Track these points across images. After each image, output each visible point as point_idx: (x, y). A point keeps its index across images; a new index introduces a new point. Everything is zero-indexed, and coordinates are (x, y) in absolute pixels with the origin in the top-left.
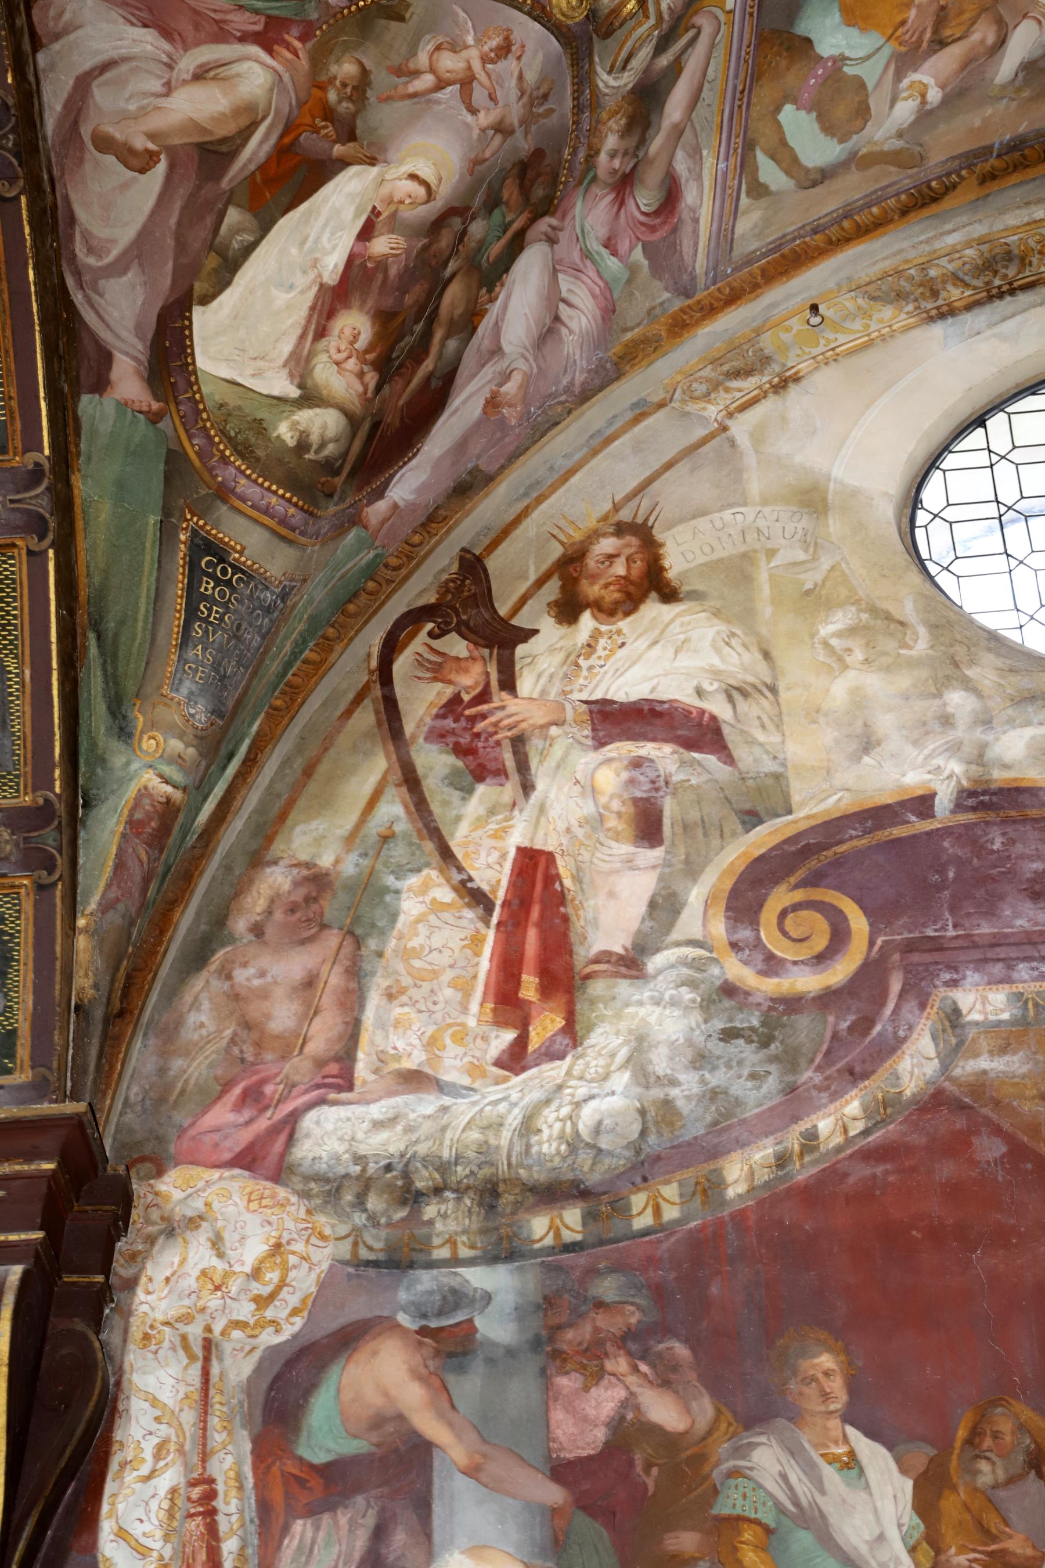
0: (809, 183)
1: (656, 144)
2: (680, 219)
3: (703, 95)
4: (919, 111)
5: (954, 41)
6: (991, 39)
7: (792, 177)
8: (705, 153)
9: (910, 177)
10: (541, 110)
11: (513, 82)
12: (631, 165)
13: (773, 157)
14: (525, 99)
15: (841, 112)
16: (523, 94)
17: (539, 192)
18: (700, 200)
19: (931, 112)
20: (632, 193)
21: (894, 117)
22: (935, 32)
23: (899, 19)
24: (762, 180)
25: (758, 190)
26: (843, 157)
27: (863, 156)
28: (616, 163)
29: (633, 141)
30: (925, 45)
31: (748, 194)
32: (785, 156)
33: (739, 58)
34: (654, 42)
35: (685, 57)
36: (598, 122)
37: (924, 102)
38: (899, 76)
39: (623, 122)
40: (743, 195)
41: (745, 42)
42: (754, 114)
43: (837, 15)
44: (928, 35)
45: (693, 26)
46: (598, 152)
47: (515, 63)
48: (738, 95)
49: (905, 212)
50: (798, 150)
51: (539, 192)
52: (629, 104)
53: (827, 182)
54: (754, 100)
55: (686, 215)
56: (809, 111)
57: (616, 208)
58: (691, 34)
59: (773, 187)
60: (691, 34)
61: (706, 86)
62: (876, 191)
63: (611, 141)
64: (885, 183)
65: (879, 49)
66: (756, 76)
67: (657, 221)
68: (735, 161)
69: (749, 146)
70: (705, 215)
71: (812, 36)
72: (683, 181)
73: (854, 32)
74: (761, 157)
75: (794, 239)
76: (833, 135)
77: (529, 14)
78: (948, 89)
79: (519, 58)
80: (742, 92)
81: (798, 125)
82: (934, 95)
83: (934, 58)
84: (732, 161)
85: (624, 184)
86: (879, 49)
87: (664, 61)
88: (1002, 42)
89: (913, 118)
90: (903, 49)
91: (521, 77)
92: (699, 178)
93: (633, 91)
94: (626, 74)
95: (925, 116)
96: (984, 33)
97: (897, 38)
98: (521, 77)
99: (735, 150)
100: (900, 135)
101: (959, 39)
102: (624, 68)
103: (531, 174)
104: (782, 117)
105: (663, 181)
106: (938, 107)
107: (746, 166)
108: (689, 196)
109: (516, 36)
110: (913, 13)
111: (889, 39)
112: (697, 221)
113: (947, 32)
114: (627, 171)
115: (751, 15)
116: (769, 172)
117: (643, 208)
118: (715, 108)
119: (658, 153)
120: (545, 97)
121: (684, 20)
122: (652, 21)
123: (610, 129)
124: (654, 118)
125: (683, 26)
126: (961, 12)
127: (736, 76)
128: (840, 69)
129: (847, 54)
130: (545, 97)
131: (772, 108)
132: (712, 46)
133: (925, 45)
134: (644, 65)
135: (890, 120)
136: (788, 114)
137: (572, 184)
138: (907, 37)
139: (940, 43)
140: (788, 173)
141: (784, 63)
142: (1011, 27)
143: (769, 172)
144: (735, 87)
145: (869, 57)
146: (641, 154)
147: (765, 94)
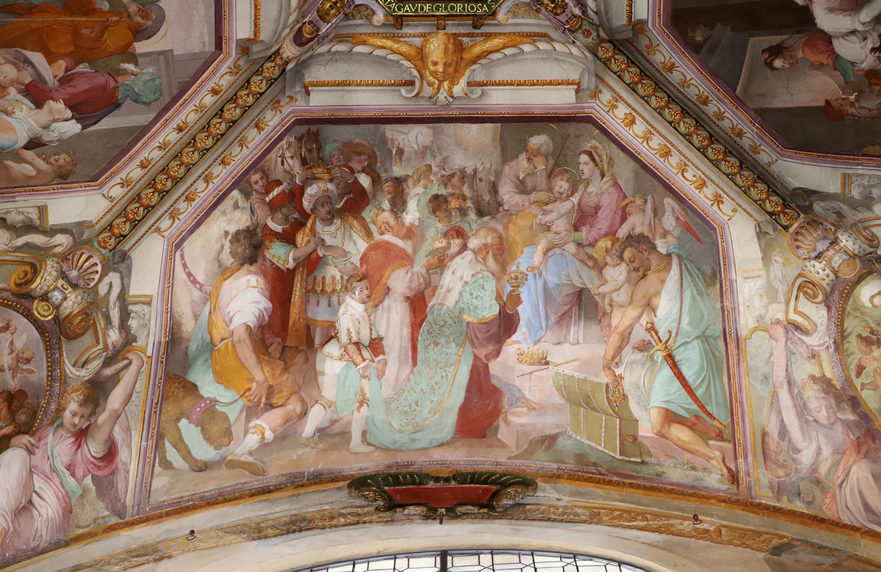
0: (196, 468)
1: (102, 418)
2: (116, 467)
3: (133, 398)
4: (261, 442)
5: (278, 407)
6: (299, 410)
7: (187, 462)
8: (133, 432)
9: (258, 480)
10: (25, 367)
11: (7, 344)
12: (86, 424)
13: (175, 447)
14: (13, 355)
15: (216, 429)
16: (12, 352)
17: (22, 418)
18: (130, 458)
19: (267, 445)
20: (86, 441)
21: (245, 444)
22: (268, 398)
23: (247, 386)
24: (168, 459)
25: (167, 465)
26: (218, 458)
27: (229, 461)
28: (76, 420)
29: (87, 411)
30: (262, 405)
31: (160, 465)
32: (180, 445)
33: (154, 384)
34: (103, 359)
35: (122, 374)
36: (65, 391)
37: (263, 438)
38: (248, 419)
39: (81, 397)
40: (157, 464)
41: (159, 376)
42: (163, 418)
43: (212, 375)
44: (263, 400)
45: (127, 358)
46: (64, 409)
47: (10, 335)
48: (154, 405)
49: (252, 495)
50: (190, 446)
51: (22, 418)
52: (87, 388)
53: (208, 471)
54: (164, 411)
55: (120, 466)
56: (197, 426)
57: (75, 447)
58: (126, 362)
59: (175, 465)
60: (126, 362)
61: (135, 394)
62: (237, 484)
63: (73, 406)
64: (243, 481)
65: (236, 401)
66: (164, 397)
67: (102, 464)
68: (152, 443)
69: (160, 437)
70: (133, 468)
71: (197, 383)
72: (119, 445)
73: (221, 387)
74: (168, 445)
75: (189, 501)
76: (211, 444)
77: (22, 314)
78: (277, 433)
79: (13, 334)
80: (157, 404)
81: (189, 431)
82: (269, 436)
83: (268, 413)
84: (150, 442)
85: (81, 435)
86: (236, 401)
87: (109, 371)
88: (304, 413)
89: (257, 445)
90: (249, 404)
91: (12, 343)
92: (129, 446)
93: (88, 381)
94: (84, 371)
95: (264, 445)
96: (294, 406)
97: (246, 397)
98: (12, 343)
99: (152, 436)
100: (250, 453)
101: (281, 406)
102: (83, 366)
103: (16, 403)
104: (180, 424)
105: (106, 441)
106: (271, 443)
107: (158, 446)
108: (123, 455)
109: (13, 324)
110: (254, 386)
111: (242, 396)
112: (128, 472)
113: (274, 401)
114: (84, 427)
115: (162, 362)
116: (172, 454)
117: (93, 454)
118: (140, 408)
119: (103, 423)
120: (28, 361)
121: (122, 353)
122: (101, 346)
123: (73, 398)
124: (101, 402)
125: (121, 356)
126: (281, 391)
127: (153, 394)
128: (214, 406)
129: (218, 399)
130: (28, 361)
131: (174, 418)
132: (139, 372)
133: (262, 405)
134: (96, 369)
135: (244, 443)
136: (183, 423)
137: (46, 422)
138: (252, 398)
139: (270, 406)
140: (184, 459)
141: (181, 394)
142: (309, 406)
143: (172, 454)
144: (152, 400)
145: (230, 404)
146: (93, 420)
147: (170, 409)
